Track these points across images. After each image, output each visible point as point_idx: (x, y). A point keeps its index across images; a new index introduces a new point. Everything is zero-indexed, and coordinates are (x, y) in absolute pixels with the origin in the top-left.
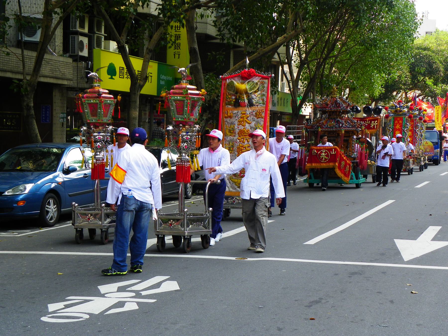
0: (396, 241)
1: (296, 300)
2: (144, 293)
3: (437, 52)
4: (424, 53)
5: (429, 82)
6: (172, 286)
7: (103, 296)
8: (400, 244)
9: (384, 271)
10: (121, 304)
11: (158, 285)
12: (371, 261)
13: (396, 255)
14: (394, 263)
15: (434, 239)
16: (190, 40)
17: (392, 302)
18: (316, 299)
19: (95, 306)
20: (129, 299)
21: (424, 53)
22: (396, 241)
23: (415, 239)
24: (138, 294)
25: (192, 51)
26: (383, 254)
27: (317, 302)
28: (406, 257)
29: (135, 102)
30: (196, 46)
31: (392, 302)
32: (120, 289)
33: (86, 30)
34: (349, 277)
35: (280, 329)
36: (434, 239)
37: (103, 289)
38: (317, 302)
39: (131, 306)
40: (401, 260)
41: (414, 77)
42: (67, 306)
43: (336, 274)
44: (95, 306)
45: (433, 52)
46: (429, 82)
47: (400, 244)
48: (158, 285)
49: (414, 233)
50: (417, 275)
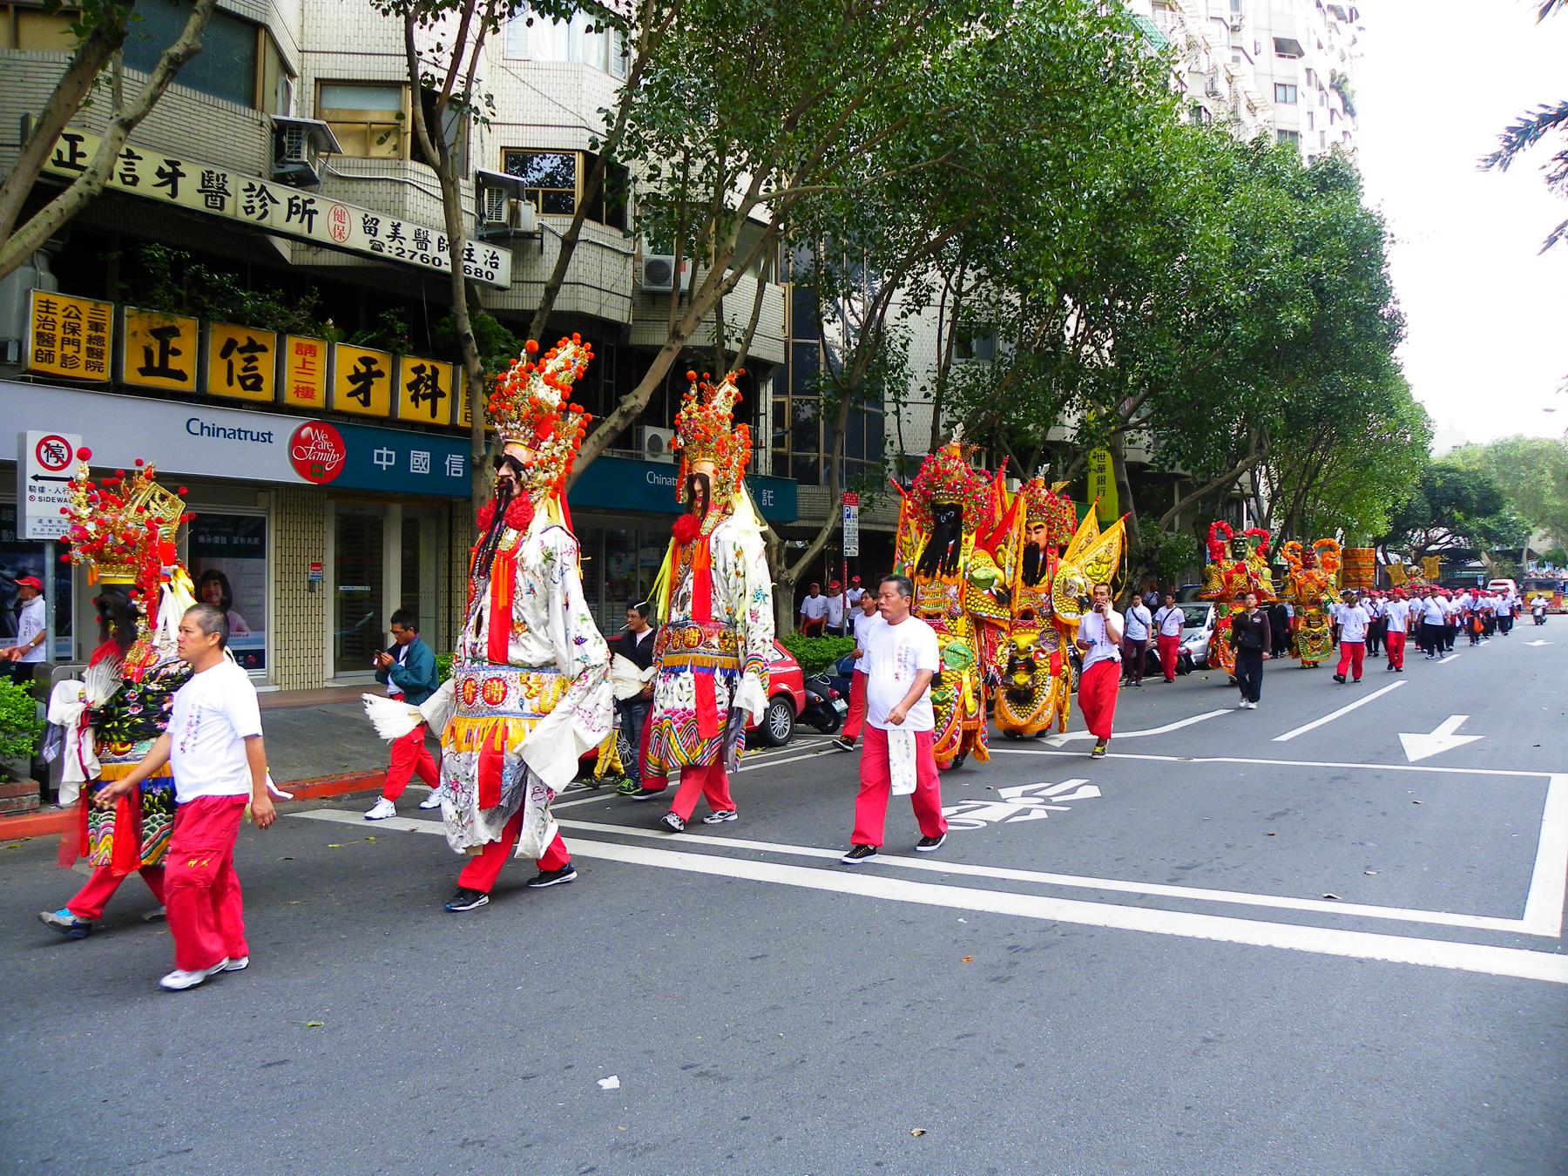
0: (1404, 737)
2: (1055, 799)
5: (1458, 515)
6: (1092, 792)
7: (1004, 801)
8: (1407, 739)
9: (1379, 776)
10: (1027, 812)
11: (1074, 790)
13: (1399, 753)
15: (1457, 733)
16: (1118, 473)
17: (1384, 814)
19: (995, 812)
22: (1404, 737)
24: (1047, 801)
25: (1120, 487)
27: (1282, 814)
28: (1412, 756)
30: (1126, 480)
31: (1384, 814)
32: (1024, 794)
33: (983, 468)
35: (1228, 846)
36: (1457, 733)
37: (1004, 793)
38: (1282, 814)
39: (1039, 814)
40: (1405, 762)
41: (1436, 510)
42: (960, 812)
44: (995, 812)
46: (1458, 515)
47: (1407, 739)
48: (1074, 790)
49: (1427, 725)
50: (1425, 781)
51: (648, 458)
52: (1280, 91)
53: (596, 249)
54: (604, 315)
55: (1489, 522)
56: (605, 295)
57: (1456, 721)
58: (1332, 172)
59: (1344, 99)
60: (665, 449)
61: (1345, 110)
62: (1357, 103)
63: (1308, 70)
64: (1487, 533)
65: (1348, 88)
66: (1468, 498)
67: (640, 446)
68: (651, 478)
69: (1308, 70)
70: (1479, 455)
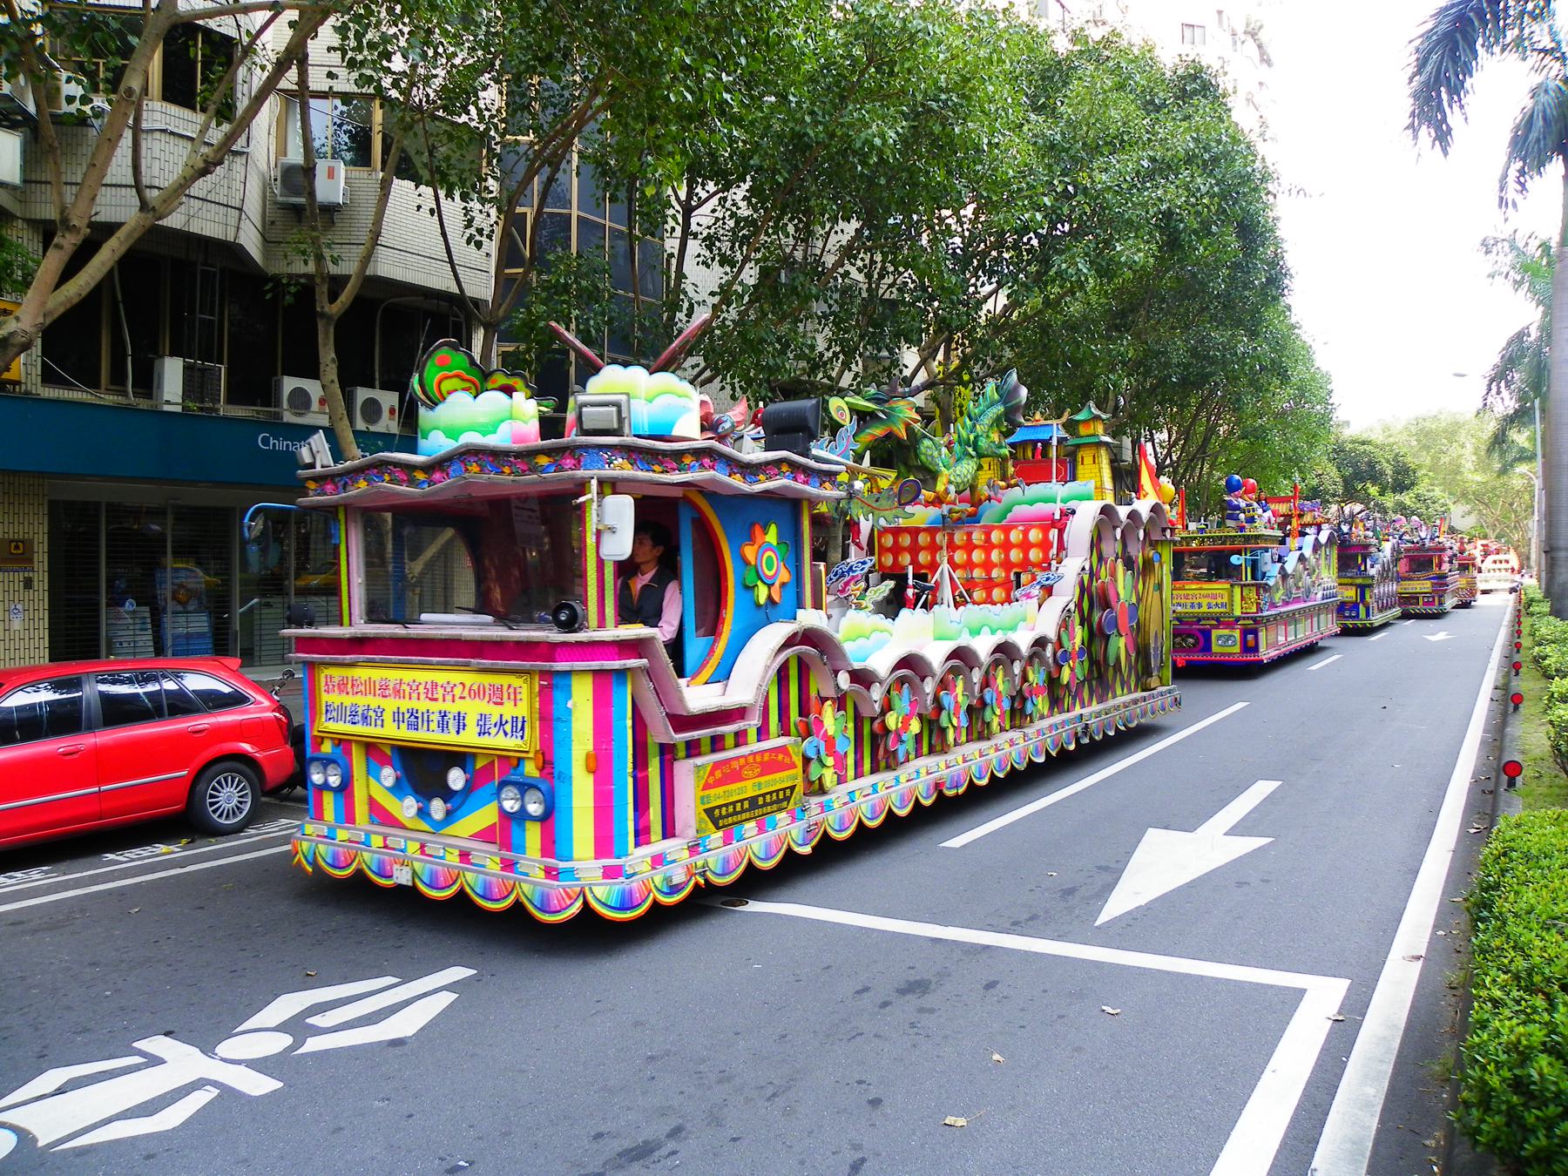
1: (599, 1136)
2: (313, 1044)
3: (1382, 447)
4: (1362, 448)
5: (1373, 490)
12: (1015, 927)
14: (1060, 938)
15: (1234, 831)
18: (656, 1130)
20: (242, 1068)
21: (1362, 448)
23: (1190, 828)
26: (1071, 891)
29: (836, 538)
34: (885, 1004)
36: (1234, 831)
41: (1347, 482)
43: (866, 989)
45: (1377, 446)
46: (1373, 490)
51: (288, 417)
52: (1188, 31)
53: (182, 142)
54: (195, 228)
55: (1407, 498)
56: (197, 203)
57: (1263, 789)
58: (1194, 78)
59: (1260, 46)
60: (315, 406)
61: (1262, 60)
62: (1271, 51)
63: (1220, 12)
64: (1402, 509)
65: (1262, 36)
66: (1382, 473)
67: (278, 404)
68: (266, 441)
69: (1220, 12)
70: (1400, 427)
